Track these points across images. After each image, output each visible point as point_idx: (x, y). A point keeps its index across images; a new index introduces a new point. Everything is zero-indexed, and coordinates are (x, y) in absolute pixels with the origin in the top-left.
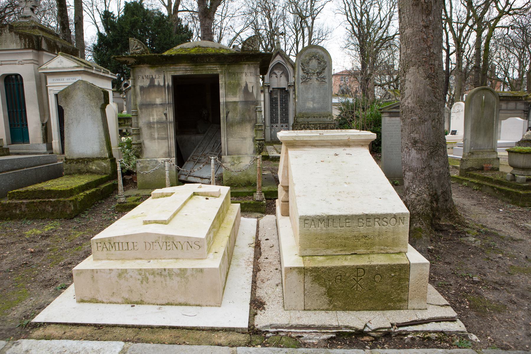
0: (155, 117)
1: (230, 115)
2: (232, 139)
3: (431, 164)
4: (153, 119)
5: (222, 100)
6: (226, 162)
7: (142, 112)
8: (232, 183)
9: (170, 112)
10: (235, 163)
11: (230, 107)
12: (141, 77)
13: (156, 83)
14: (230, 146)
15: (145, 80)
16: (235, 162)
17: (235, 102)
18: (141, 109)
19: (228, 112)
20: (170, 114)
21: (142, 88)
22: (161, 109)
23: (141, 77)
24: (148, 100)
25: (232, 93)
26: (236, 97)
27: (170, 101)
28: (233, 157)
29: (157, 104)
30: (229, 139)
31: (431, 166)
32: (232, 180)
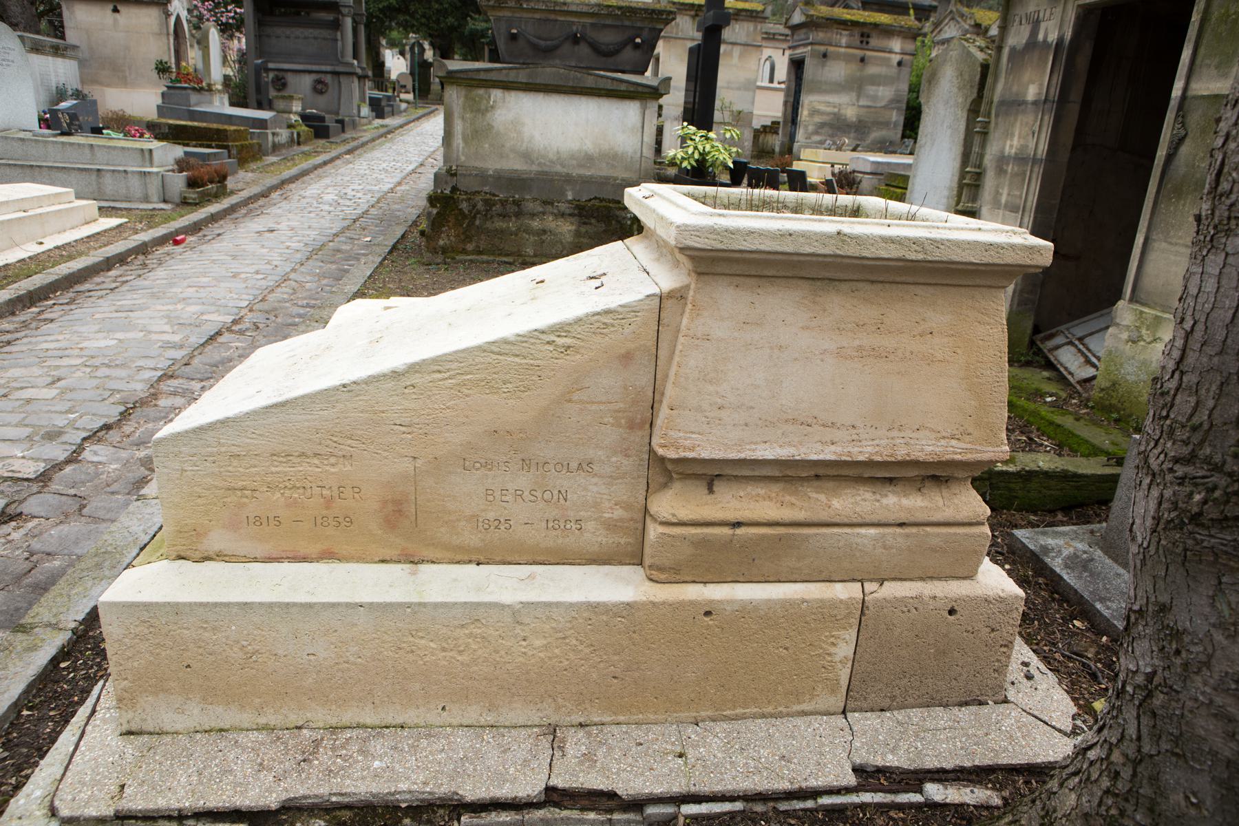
0: (1015, 142)
1: (1184, 150)
2: (1164, 245)
3: (1183, 622)
4: (1011, 146)
5: (1176, 92)
6: (1118, 325)
7: (996, 124)
8: (1114, 402)
9: (1044, 129)
10: (1140, 338)
11: (1195, 119)
12: (1017, 19)
13: (1041, 37)
14: (1150, 268)
15: (1023, 27)
16: (1144, 331)
17: (1216, 96)
18: (997, 116)
19: (1182, 140)
20: (1043, 135)
21: (1013, 50)
22: (1030, 118)
23: (1017, 19)
24: (1015, 89)
25: (1217, 60)
26: (1225, 76)
27: (1052, 91)
28: (1141, 312)
29: (1024, 102)
30: (1156, 245)
31: (1177, 634)
32: (1114, 394)
